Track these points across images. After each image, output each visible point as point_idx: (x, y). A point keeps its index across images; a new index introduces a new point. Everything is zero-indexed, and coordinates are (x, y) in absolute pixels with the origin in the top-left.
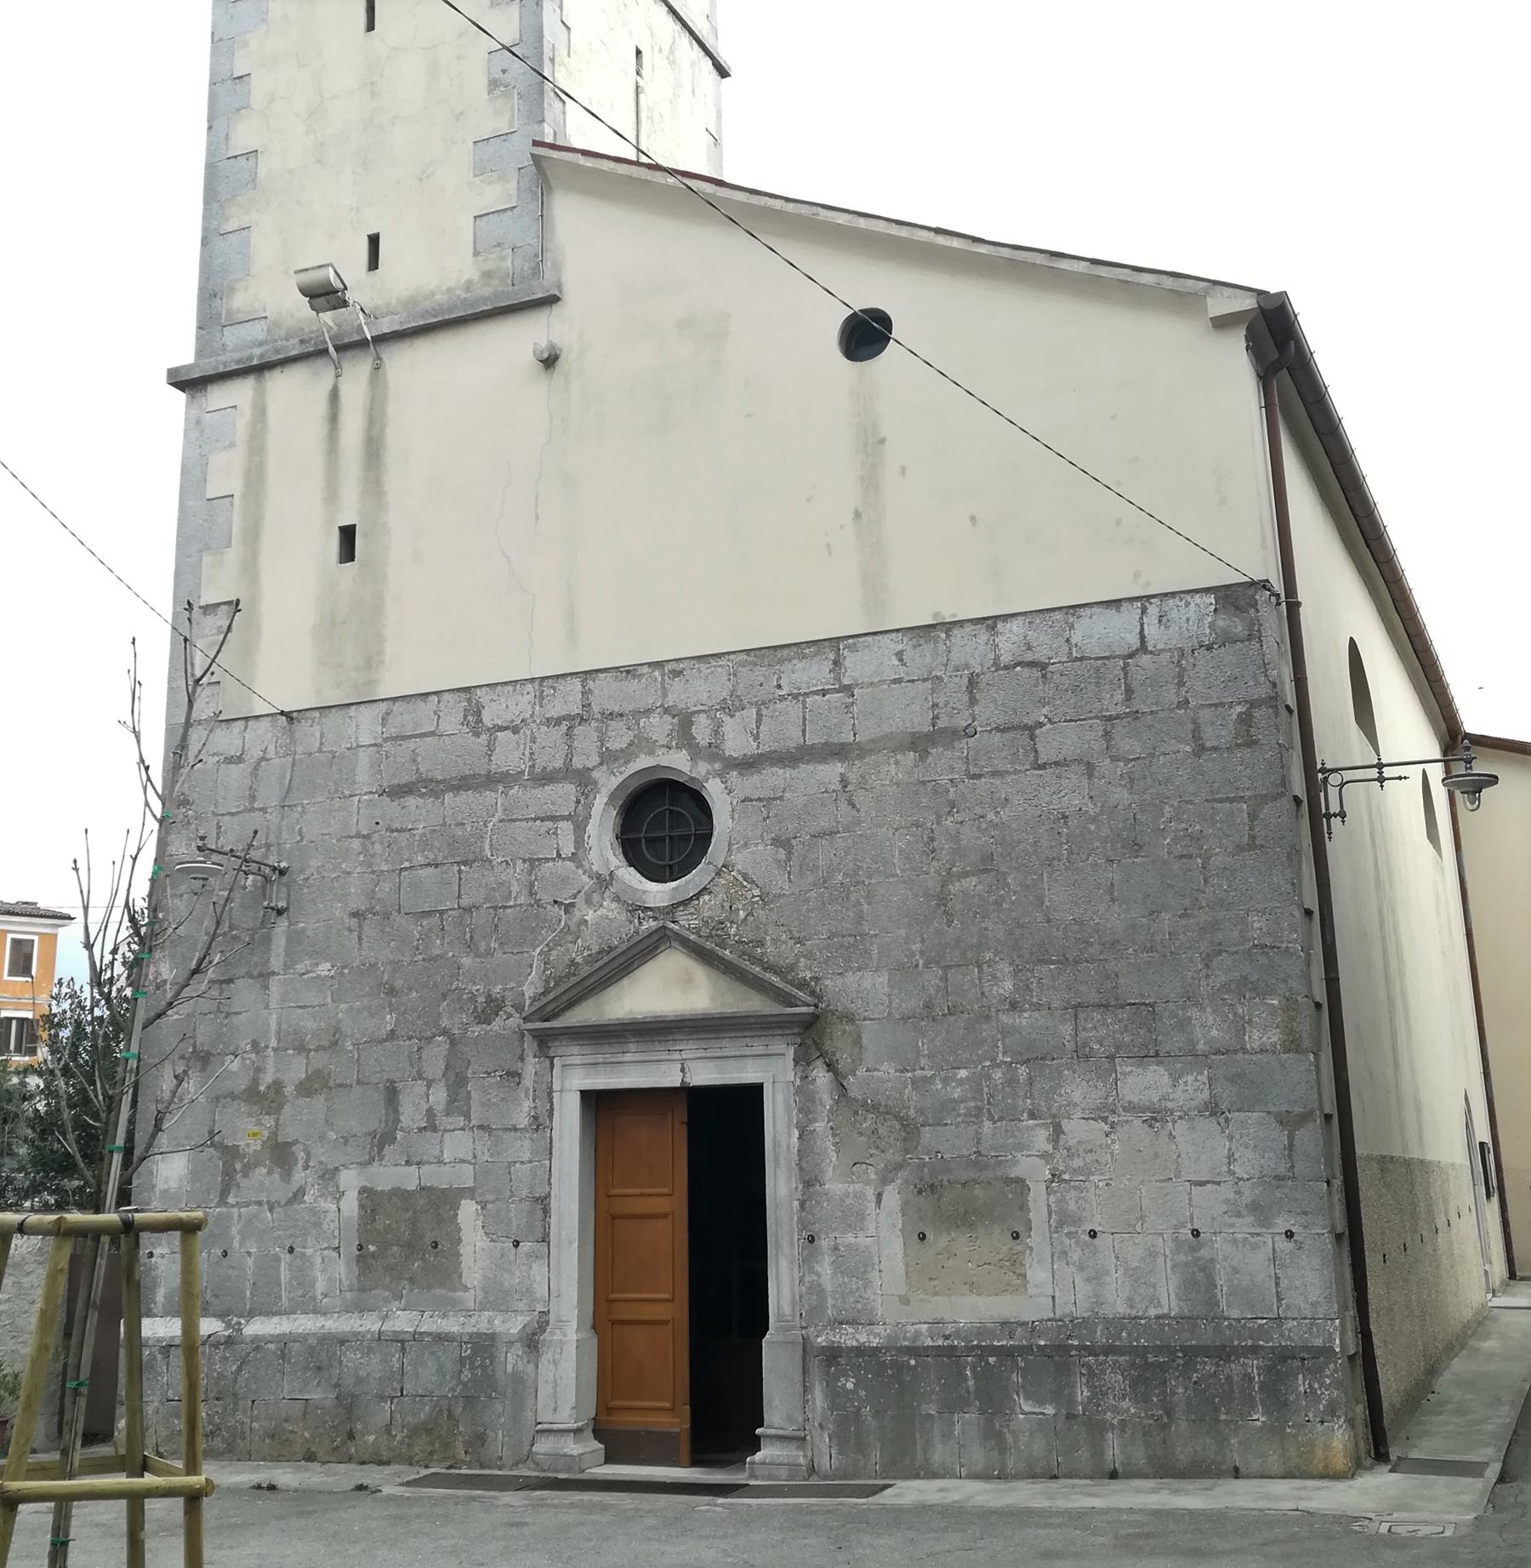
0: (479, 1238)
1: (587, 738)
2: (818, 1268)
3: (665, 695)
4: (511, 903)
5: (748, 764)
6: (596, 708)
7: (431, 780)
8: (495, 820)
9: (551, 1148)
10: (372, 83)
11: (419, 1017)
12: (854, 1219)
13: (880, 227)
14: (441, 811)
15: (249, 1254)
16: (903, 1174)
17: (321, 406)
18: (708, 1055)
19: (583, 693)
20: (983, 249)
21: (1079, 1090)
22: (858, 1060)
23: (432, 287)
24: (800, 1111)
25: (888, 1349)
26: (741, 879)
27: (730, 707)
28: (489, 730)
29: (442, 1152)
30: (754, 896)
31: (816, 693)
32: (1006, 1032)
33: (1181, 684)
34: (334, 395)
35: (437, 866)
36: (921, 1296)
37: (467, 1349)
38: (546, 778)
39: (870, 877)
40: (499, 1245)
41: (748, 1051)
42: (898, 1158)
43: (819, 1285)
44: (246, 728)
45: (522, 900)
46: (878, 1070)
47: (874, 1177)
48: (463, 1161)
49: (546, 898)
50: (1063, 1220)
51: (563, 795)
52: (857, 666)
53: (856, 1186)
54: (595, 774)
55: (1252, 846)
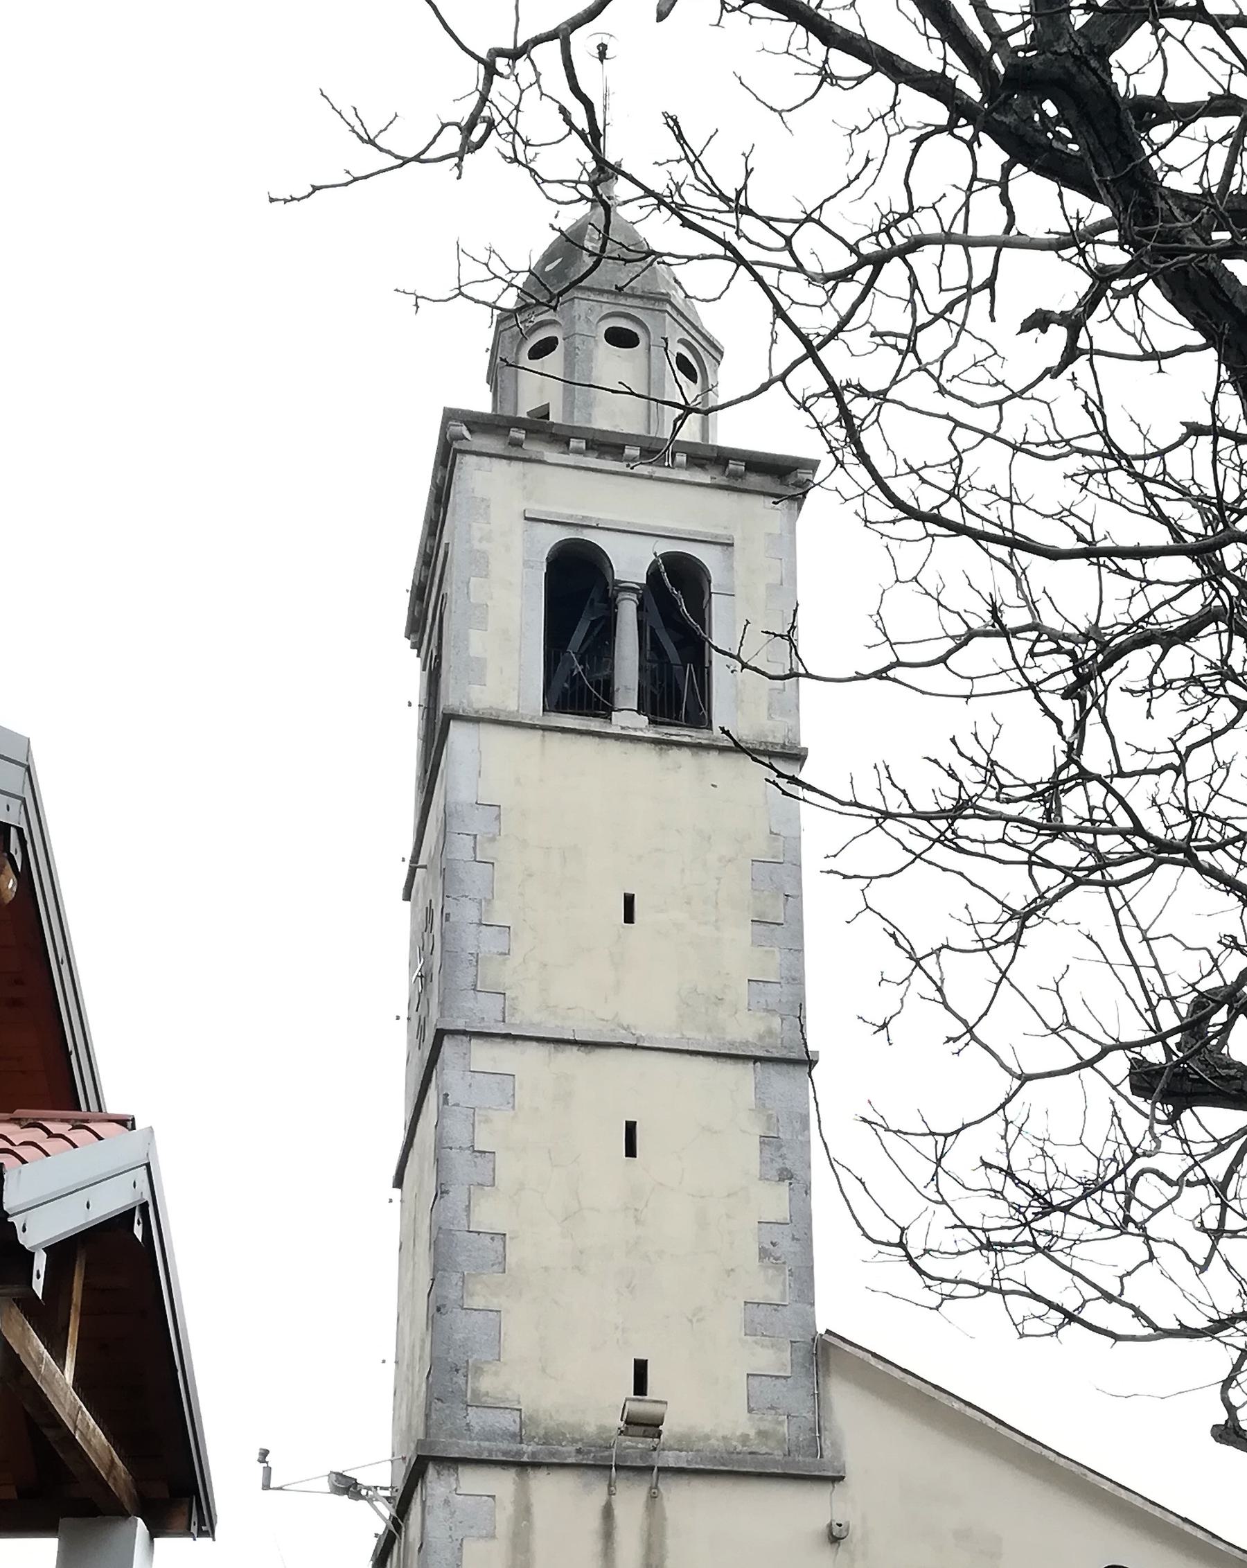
10: (636, 1210)
13: (1139, 1502)
17: (594, 1521)
23: (707, 1430)
34: (608, 1513)
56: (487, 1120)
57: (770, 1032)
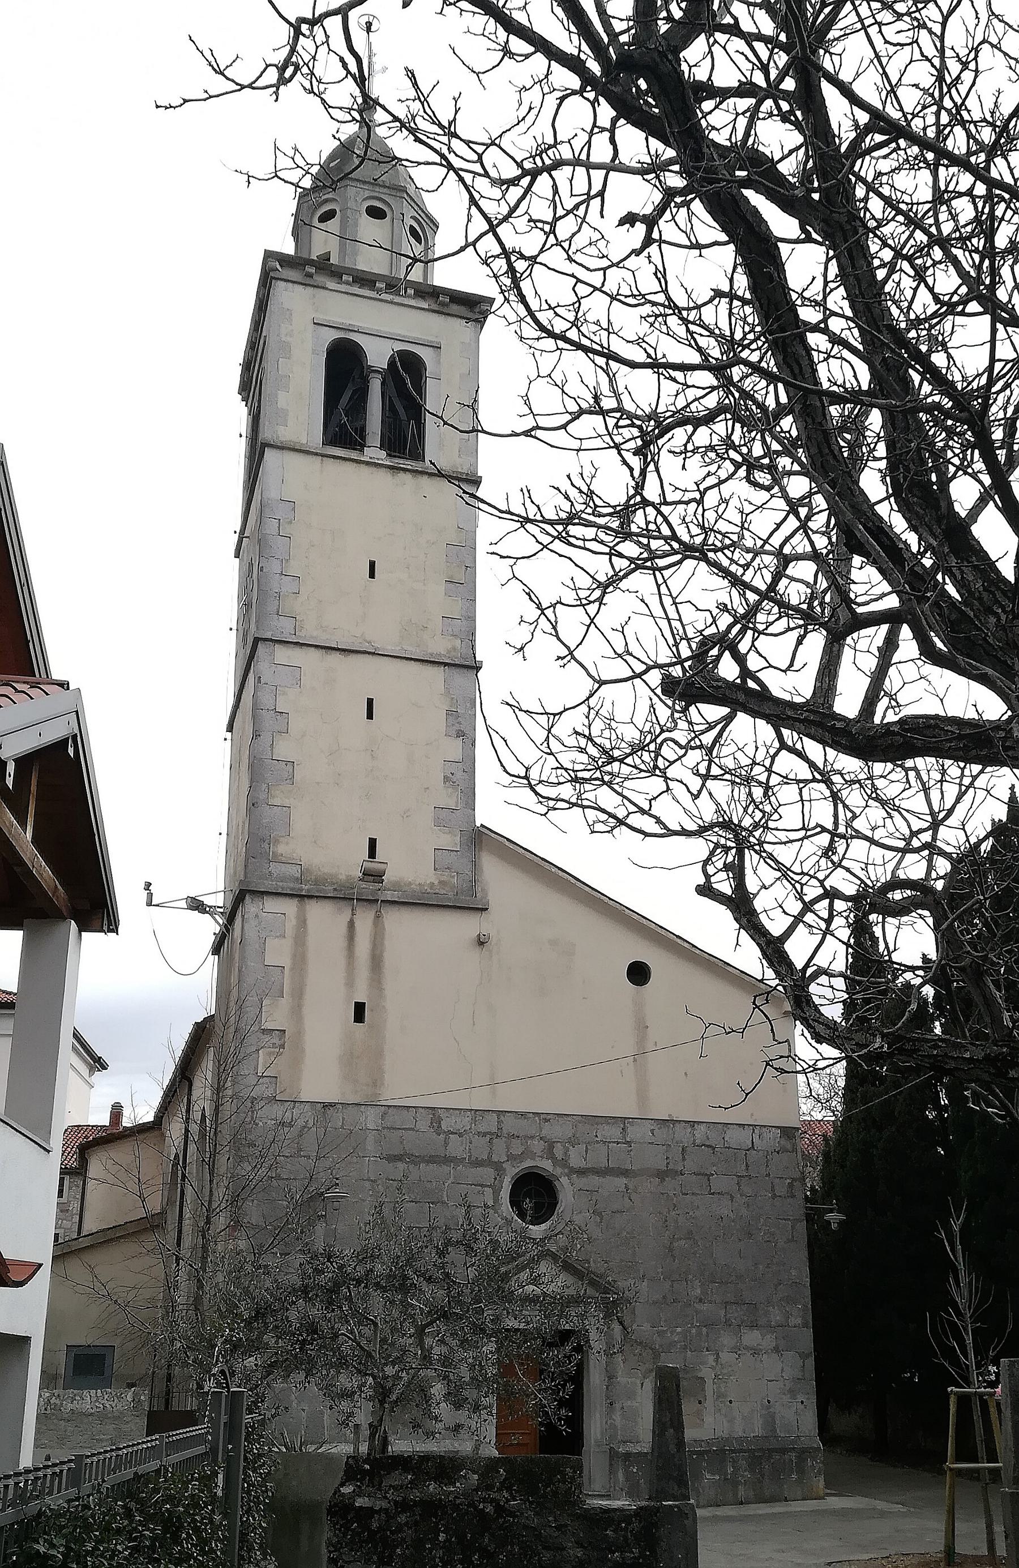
1: (499, 1144)
2: (614, 1417)
5: (582, 1172)
6: (505, 1131)
12: (631, 1395)
15: (303, 1410)
20: (698, 952)
21: (727, 1340)
22: (633, 1321)
27: (573, 1141)
28: (445, 1132)
31: (614, 1142)
32: (697, 1312)
33: (767, 1166)
34: (351, 925)
38: (478, 1163)
44: (294, 1107)
50: (719, 1396)
51: (487, 1174)
52: (634, 1133)
55: (793, 1240)
56: (284, 693)
57: (454, 649)
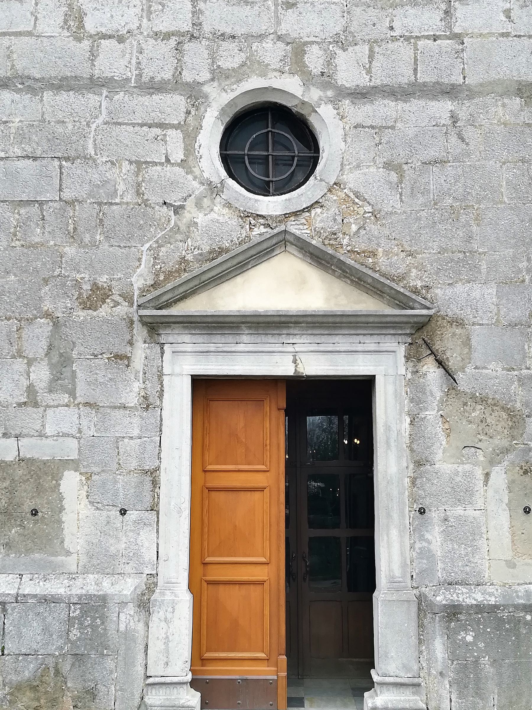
0: (82, 506)
2: (428, 536)
3: (278, 23)
4: (117, 200)
6: (207, 28)
7: (29, 78)
8: (100, 121)
9: (161, 425)
11: (18, 299)
14: (40, 107)
16: (511, 456)
18: (322, 349)
19: (193, 13)
22: (467, 359)
24: (412, 400)
25: (505, 606)
26: (353, 196)
28: (91, 36)
29: (43, 426)
30: (365, 212)
31: (428, 37)
35: (35, 159)
36: (526, 560)
37: (75, 610)
39: (479, 202)
40: (104, 513)
41: (360, 348)
42: (505, 443)
43: (429, 551)
45: (129, 198)
46: (486, 368)
47: (482, 459)
48: (67, 435)
49: (154, 199)
53: (465, 466)
54: (206, 89)
